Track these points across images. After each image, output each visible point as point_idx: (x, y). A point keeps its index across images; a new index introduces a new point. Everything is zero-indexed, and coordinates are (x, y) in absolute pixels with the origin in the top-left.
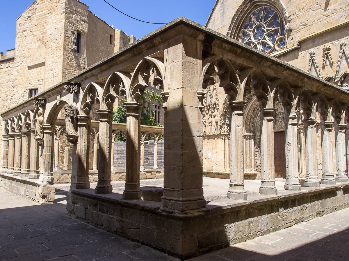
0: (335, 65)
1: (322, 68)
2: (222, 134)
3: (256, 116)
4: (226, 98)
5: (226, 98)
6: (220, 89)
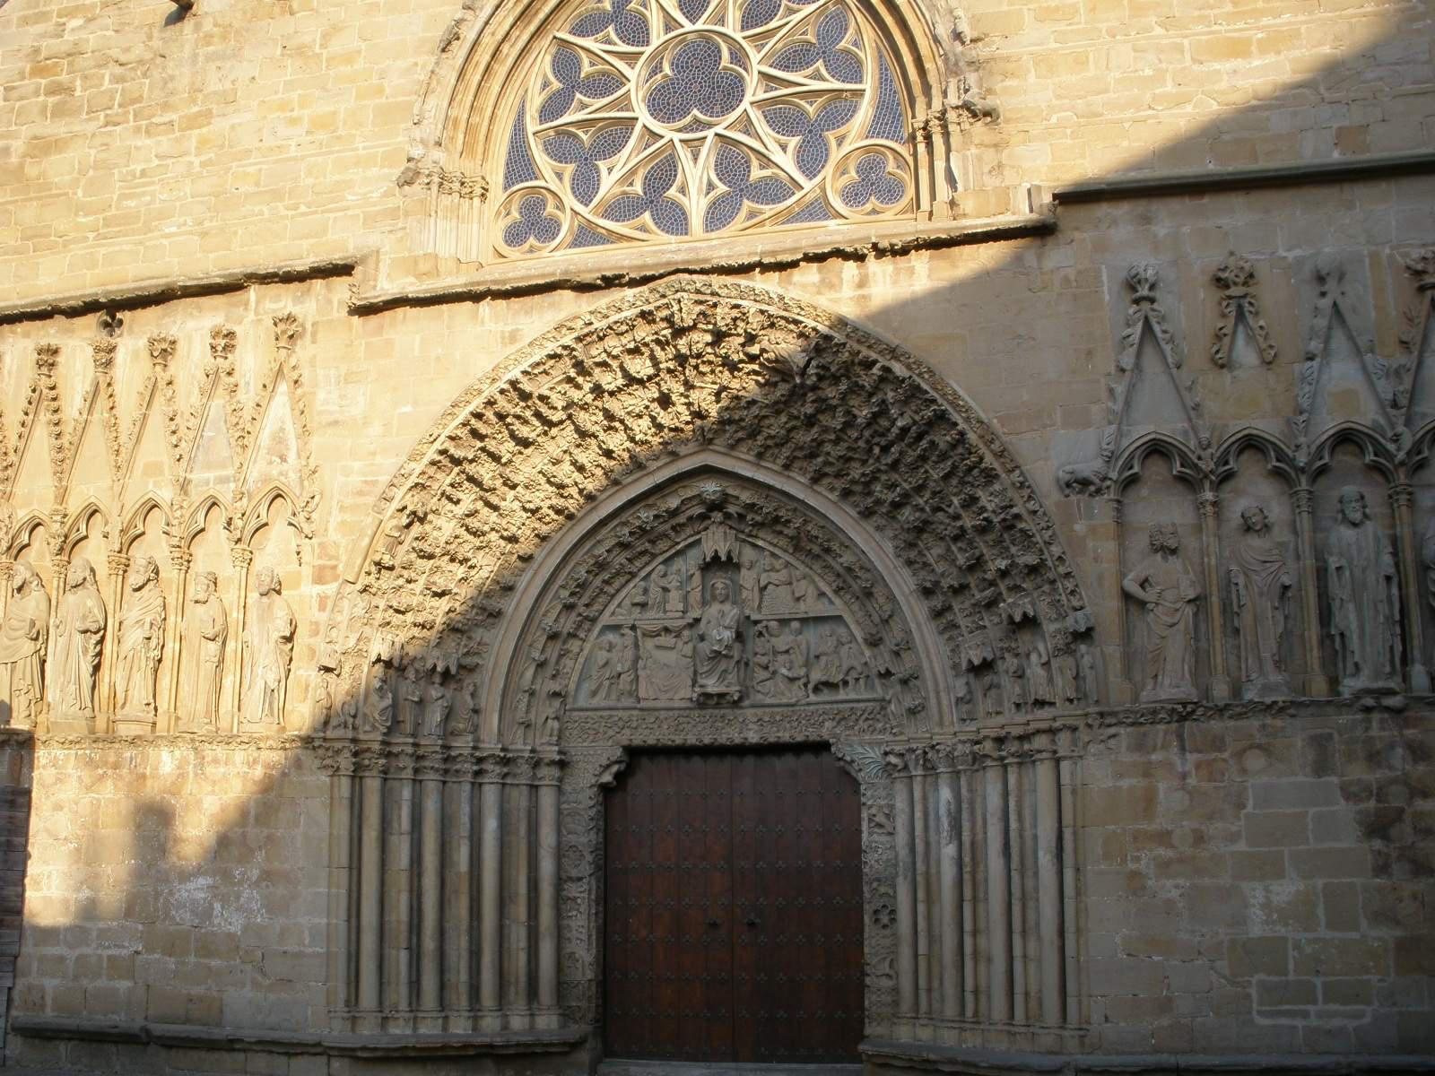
3: (586, 625)
6: (342, 397)
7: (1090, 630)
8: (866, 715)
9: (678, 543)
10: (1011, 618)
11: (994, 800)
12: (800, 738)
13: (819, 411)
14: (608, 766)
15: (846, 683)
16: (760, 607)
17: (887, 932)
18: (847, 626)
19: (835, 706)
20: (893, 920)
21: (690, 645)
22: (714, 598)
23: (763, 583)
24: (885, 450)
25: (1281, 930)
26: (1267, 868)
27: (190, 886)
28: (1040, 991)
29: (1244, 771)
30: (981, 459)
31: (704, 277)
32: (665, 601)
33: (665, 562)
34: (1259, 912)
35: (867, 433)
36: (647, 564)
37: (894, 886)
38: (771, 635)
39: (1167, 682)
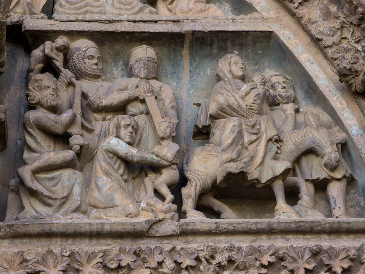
15: (293, 196)
18: (284, 56)
19: (264, 242)
38: (80, 75)
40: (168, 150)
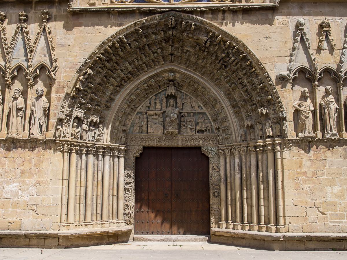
0: (337, 52)
1: (315, 52)
2: (61, 139)
4: (88, 61)
5: (88, 61)
6: (65, 38)
7: (286, 116)
8: (212, 139)
9: (160, 90)
10: (262, 113)
11: (253, 162)
12: (193, 145)
13: (207, 55)
14: (139, 151)
15: (206, 130)
16: (182, 109)
17: (217, 198)
18: (206, 114)
20: (219, 195)
21: (162, 118)
22: (170, 105)
23: (183, 103)
24: (226, 67)
25: (336, 200)
26: (331, 183)
27: (11, 186)
28: (269, 215)
29: (326, 157)
30: (255, 70)
31: (179, 13)
32: (155, 106)
33: (155, 95)
34: (330, 195)
35: (221, 62)
36: (151, 95)
37: (219, 186)
39: (307, 132)
40: (195, 127)
